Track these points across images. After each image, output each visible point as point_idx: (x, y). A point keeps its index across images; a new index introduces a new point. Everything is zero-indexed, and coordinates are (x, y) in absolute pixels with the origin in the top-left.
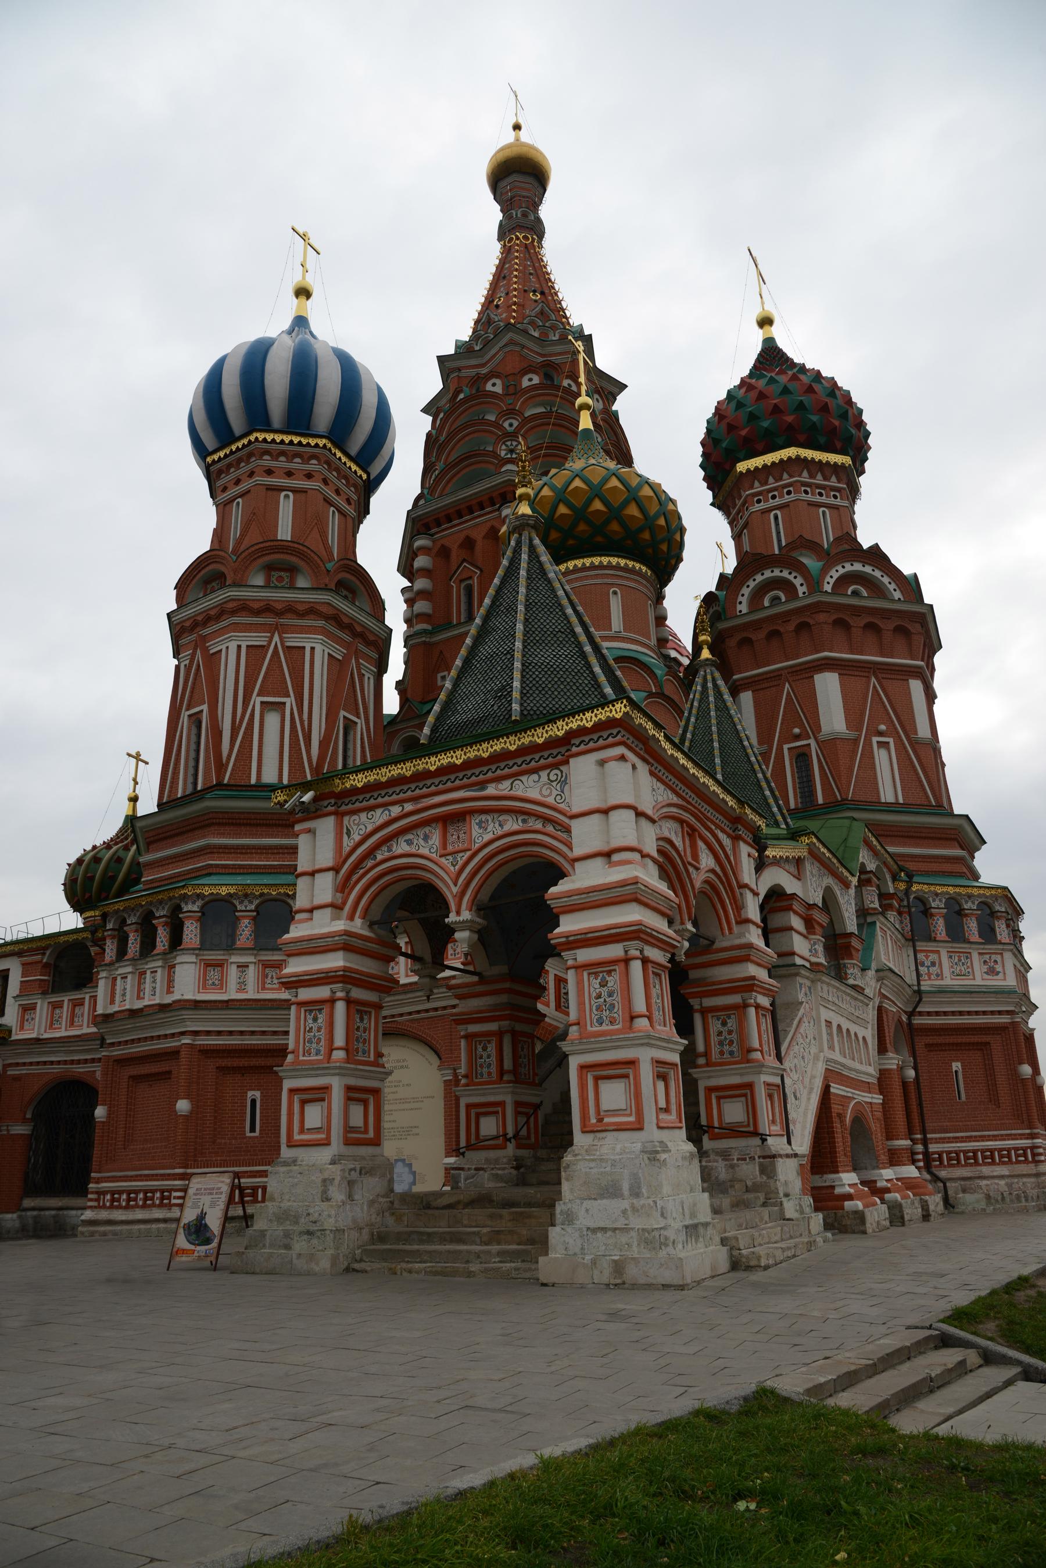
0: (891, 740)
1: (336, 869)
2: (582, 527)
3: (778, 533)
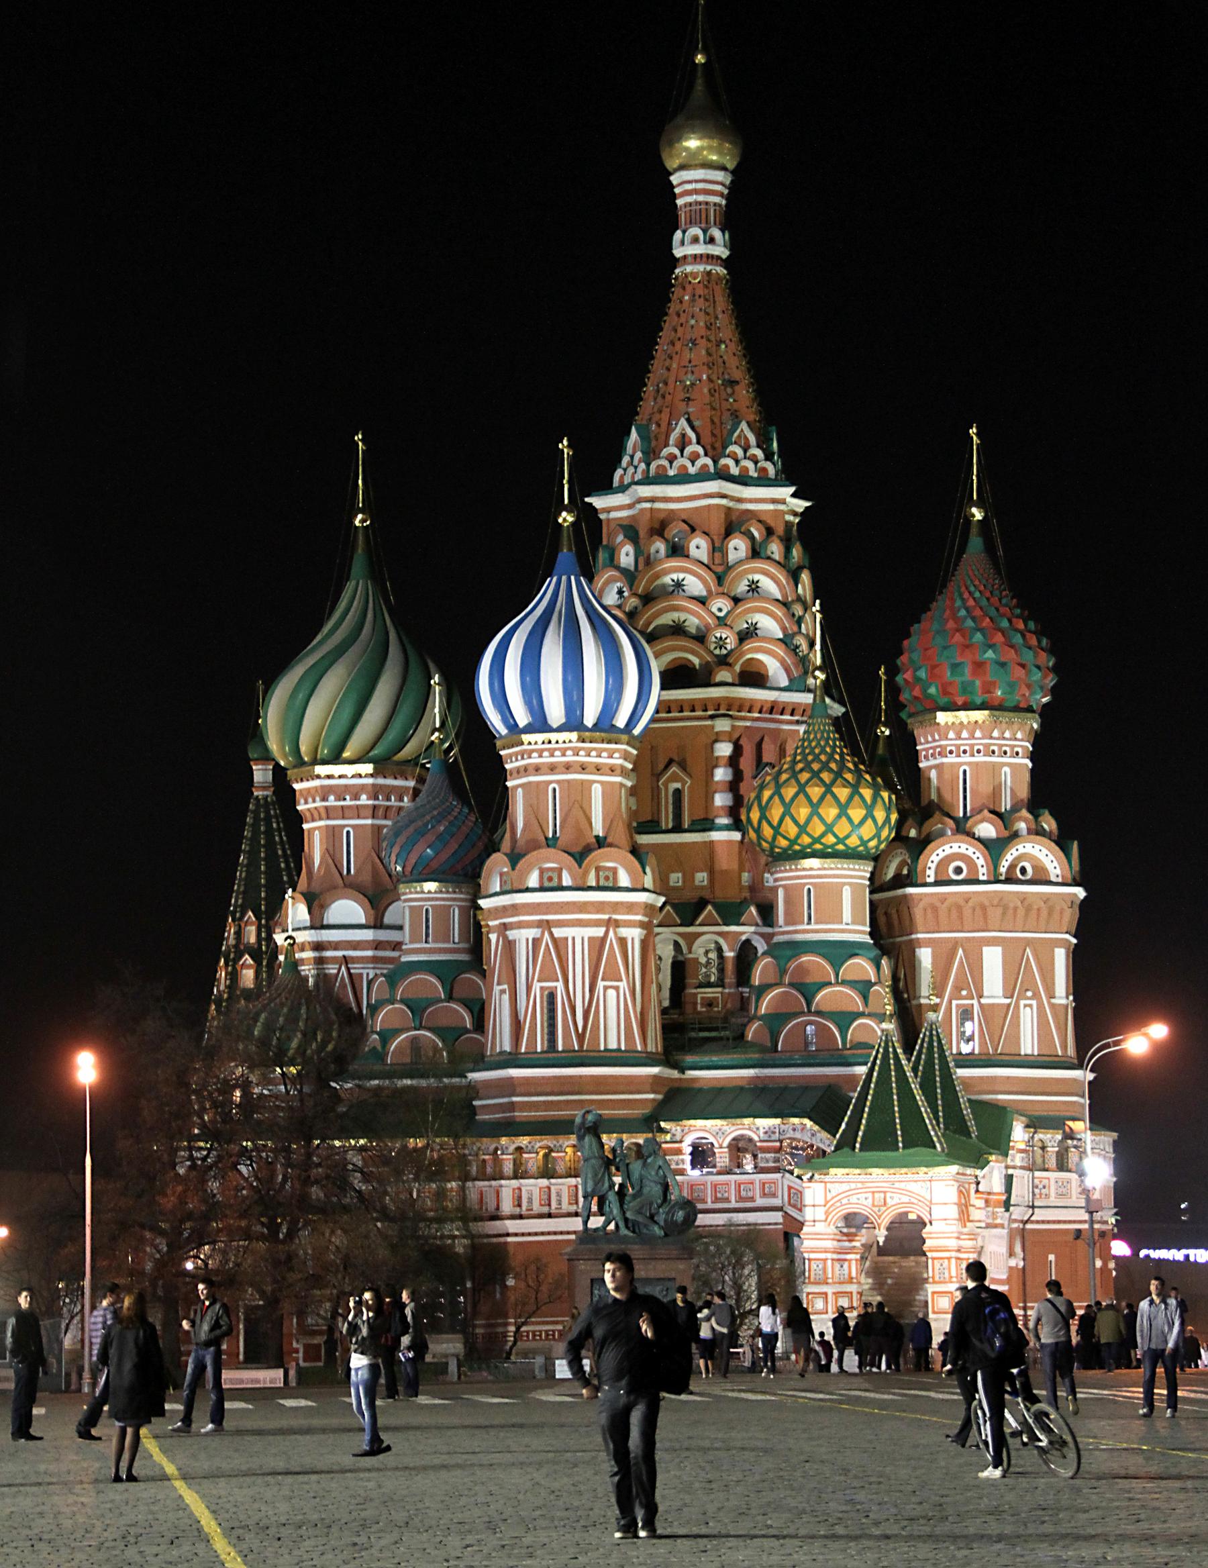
0: (1034, 1003)
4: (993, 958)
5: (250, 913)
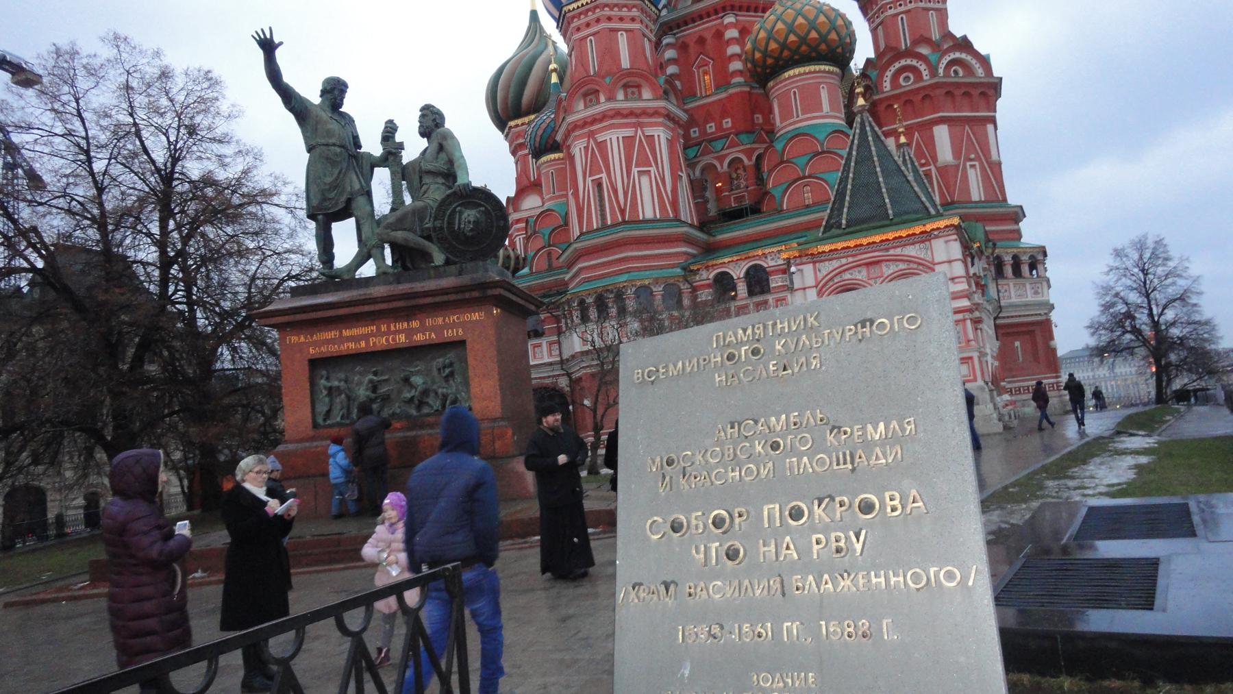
1: (816, 287)
2: (804, 48)
3: (904, 29)
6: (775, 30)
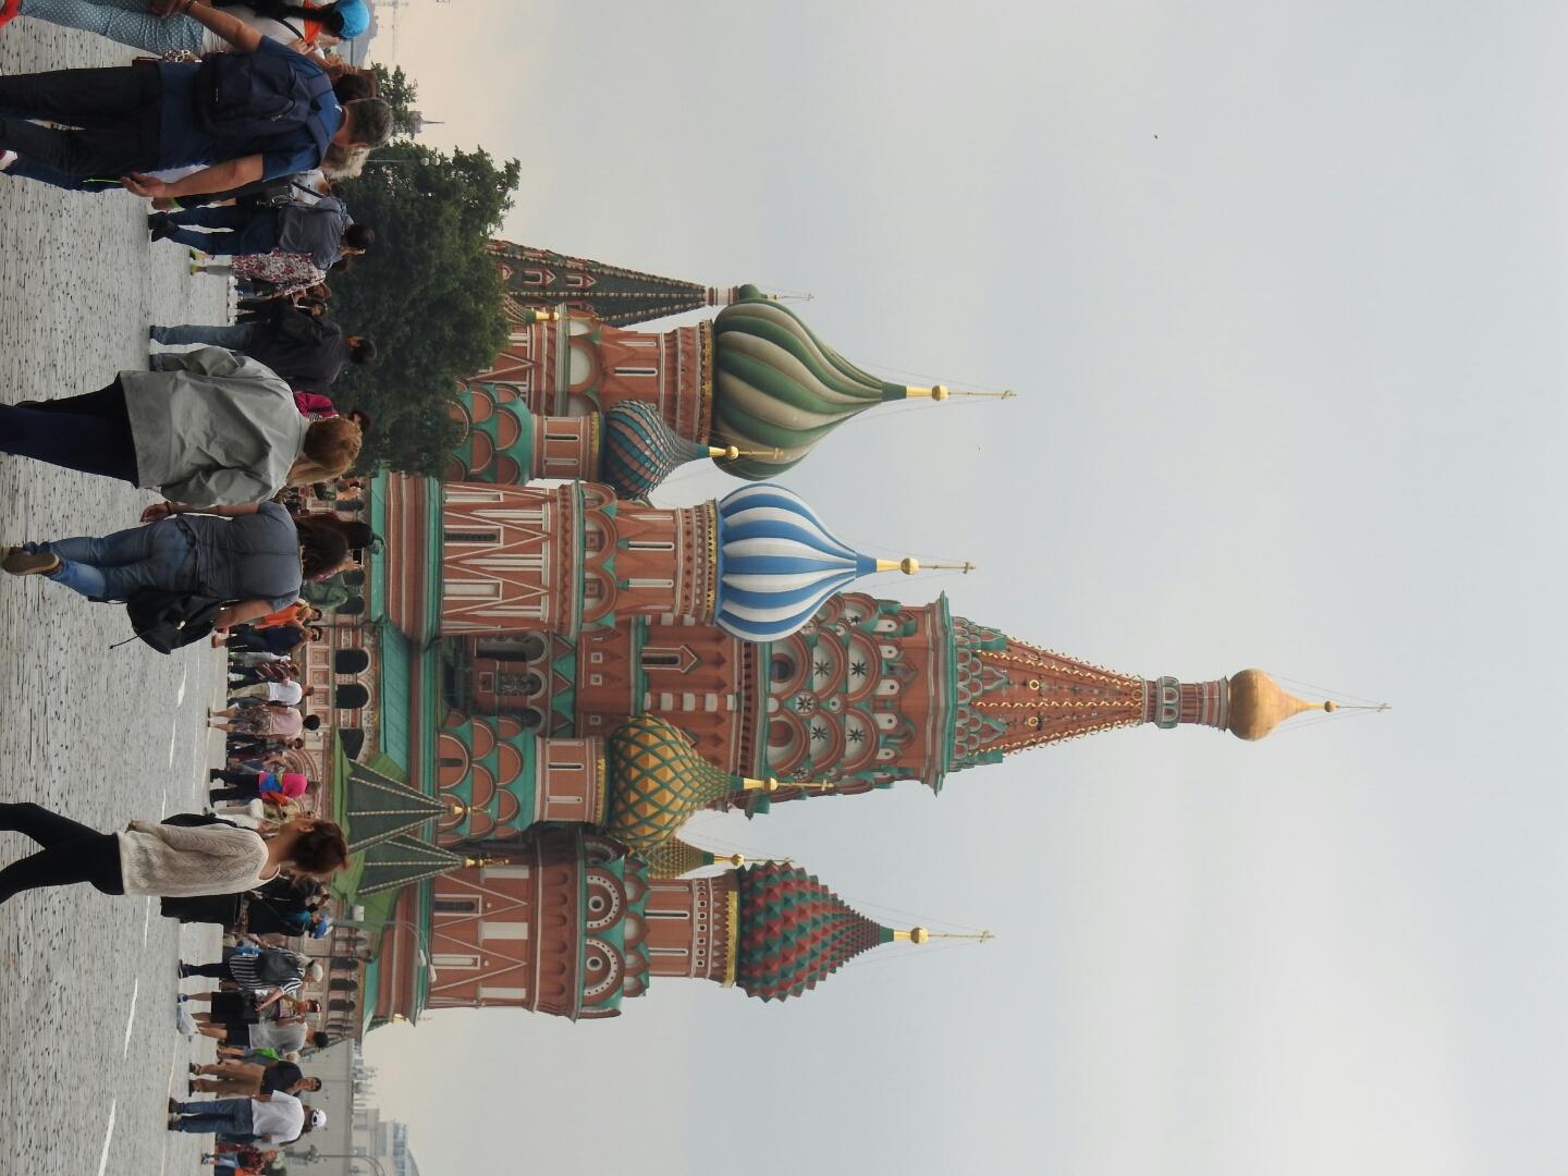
0: (478, 968)
4: (517, 931)
5: (595, 282)
6: (650, 755)
